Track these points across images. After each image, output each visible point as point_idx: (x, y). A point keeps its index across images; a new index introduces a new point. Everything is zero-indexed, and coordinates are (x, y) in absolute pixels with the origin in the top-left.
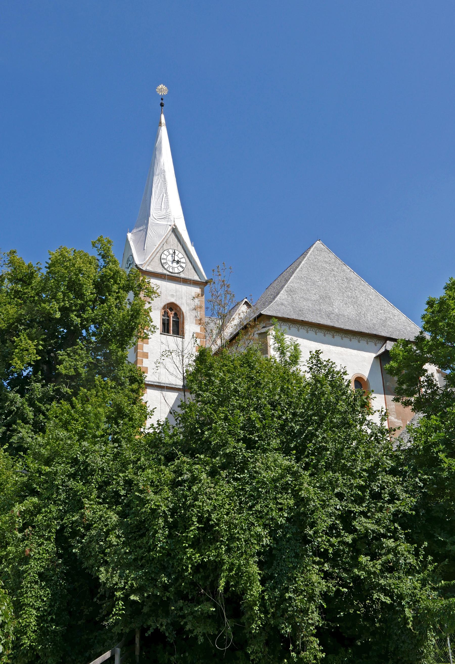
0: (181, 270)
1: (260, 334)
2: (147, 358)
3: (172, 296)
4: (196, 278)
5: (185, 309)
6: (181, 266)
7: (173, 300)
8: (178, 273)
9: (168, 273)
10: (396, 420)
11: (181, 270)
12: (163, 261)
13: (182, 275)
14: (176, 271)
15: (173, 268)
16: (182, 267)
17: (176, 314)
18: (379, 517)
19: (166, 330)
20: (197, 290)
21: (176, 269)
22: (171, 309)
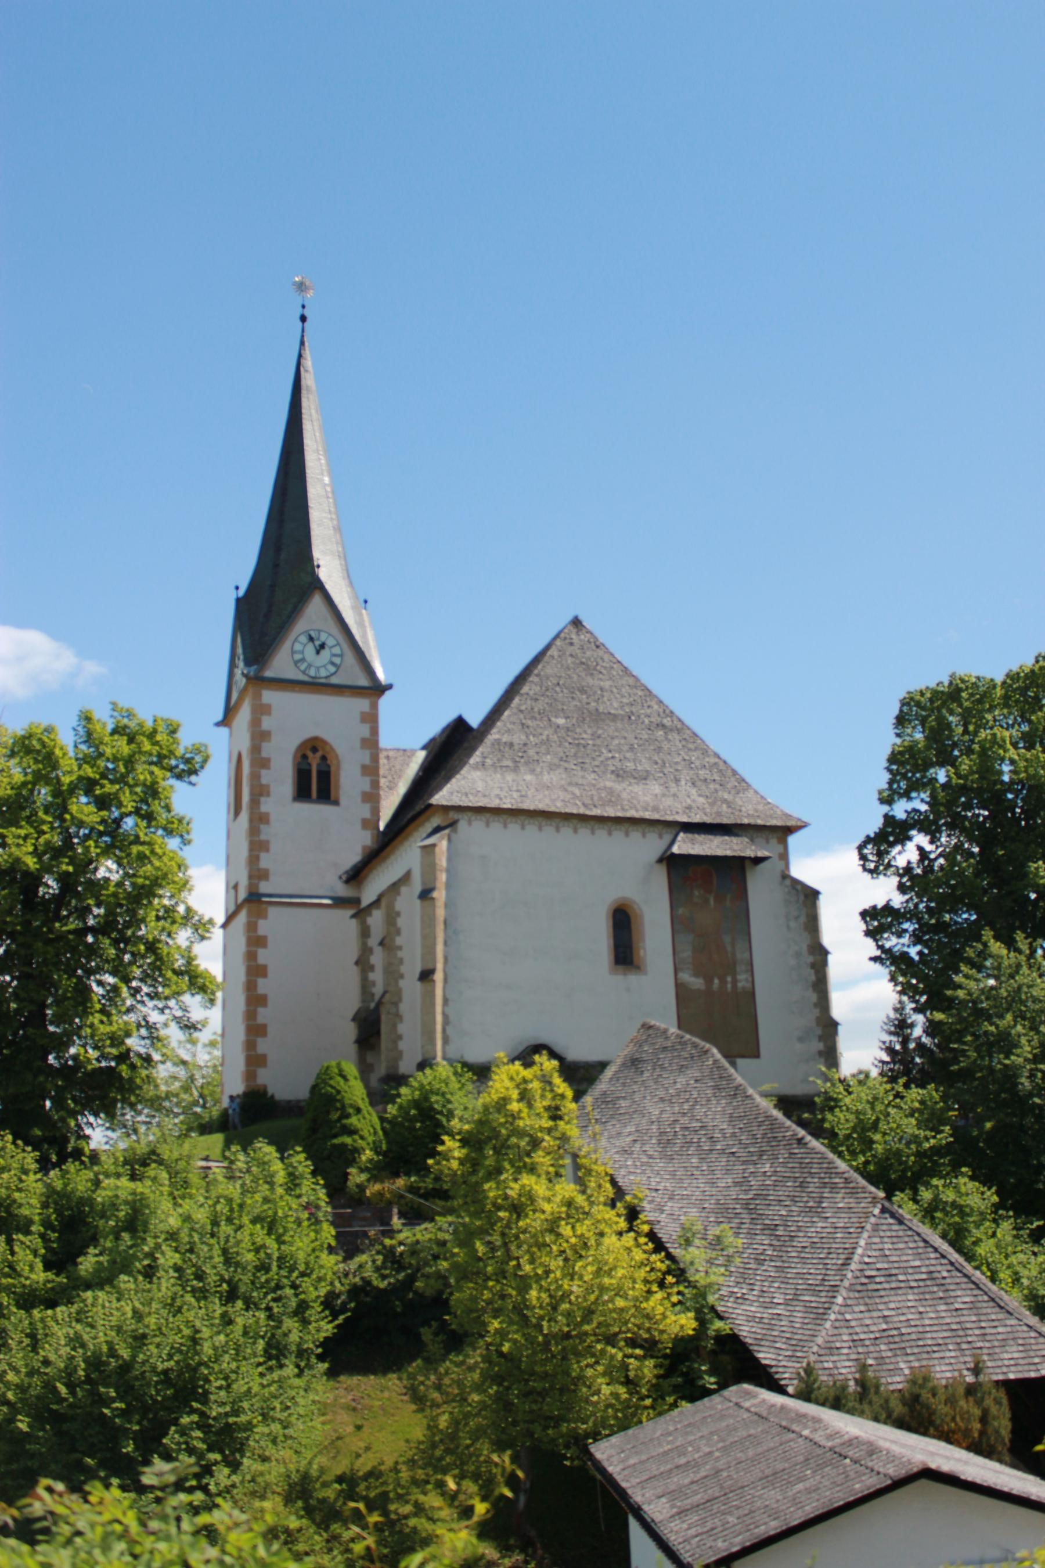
0: (332, 669)
1: (424, 847)
2: (267, 850)
4: (363, 681)
6: (333, 664)
8: (326, 677)
9: (305, 678)
10: (693, 979)
11: (332, 669)
13: (334, 680)
14: (323, 673)
15: (318, 668)
16: (333, 664)
18: (970, 994)
22: (314, 750)
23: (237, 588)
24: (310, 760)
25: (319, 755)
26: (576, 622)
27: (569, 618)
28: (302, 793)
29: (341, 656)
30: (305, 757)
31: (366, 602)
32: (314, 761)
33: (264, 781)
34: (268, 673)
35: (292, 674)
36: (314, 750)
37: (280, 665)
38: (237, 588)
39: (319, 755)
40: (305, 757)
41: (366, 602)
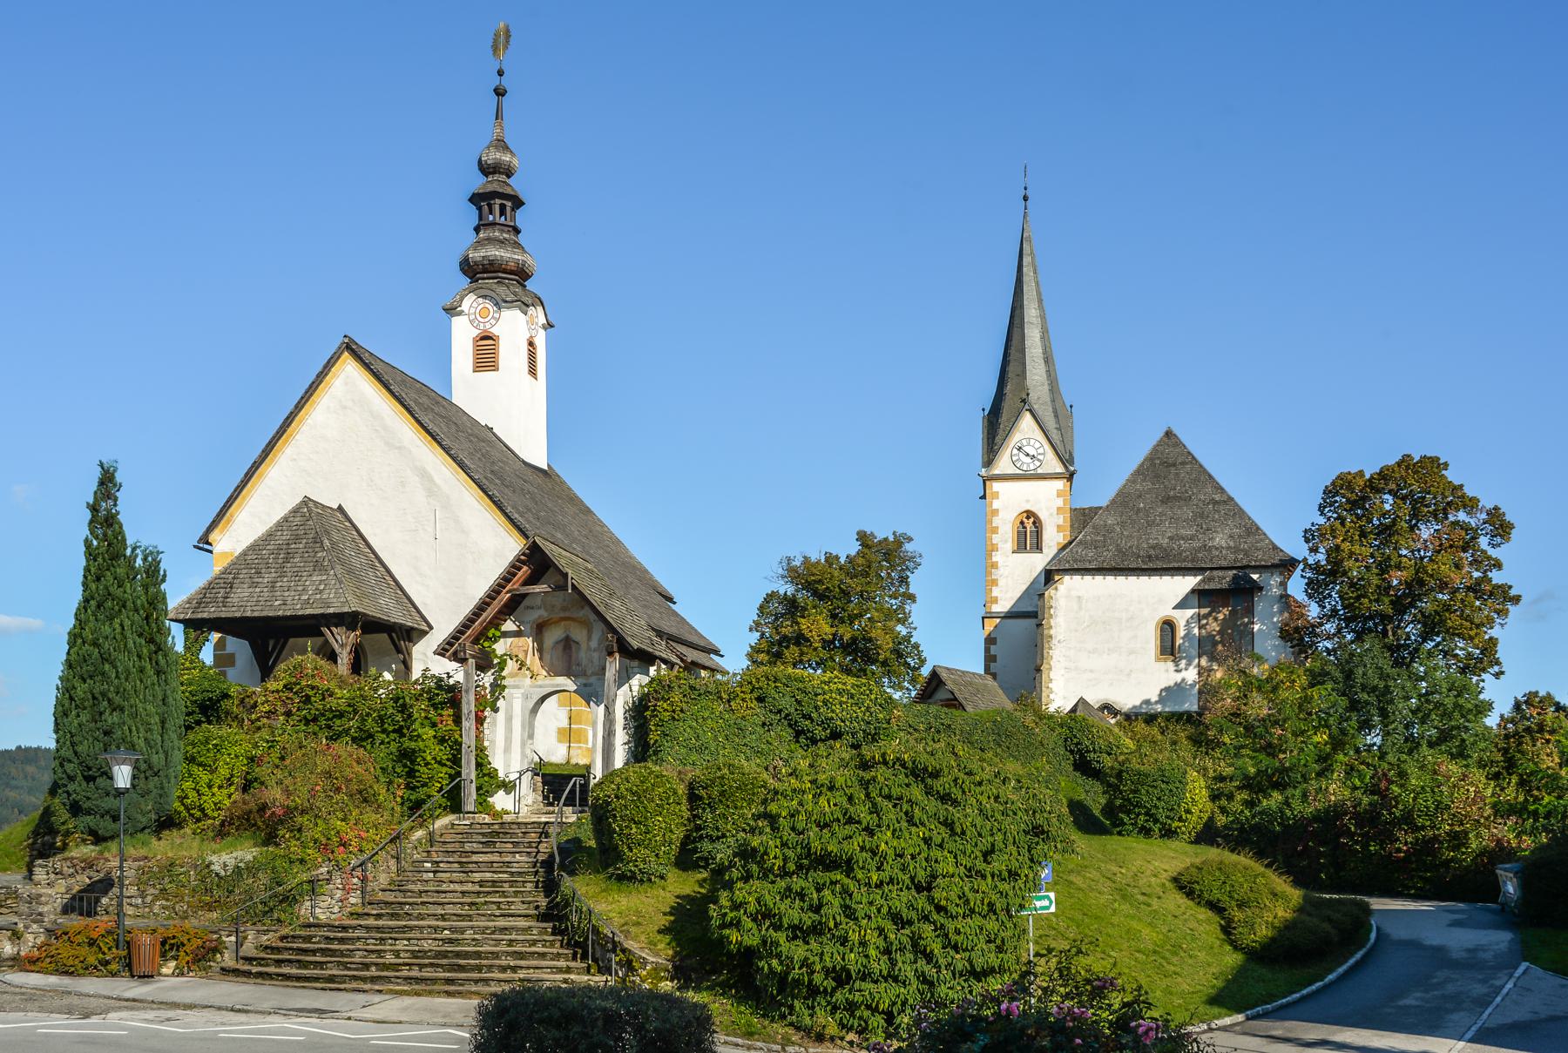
0: (1038, 464)
2: (997, 585)
3: (1028, 501)
5: (1042, 516)
7: (1028, 507)
9: (1021, 472)
11: (1038, 464)
12: (1014, 458)
13: (1040, 471)
14: (1032, 467)
16: (1038, 460)
17: (1034, 523)
19: (1021, 547)
20: (1060, 484)
21: (1028, 465)
22: (1028, 518)
23: (983, 410)
24: (1026, 525)
25: (1032, 520)
26: (1169, 434)
27: (1165, 429)
28: (1021, 547)
29: (1044, 454)
30: (1022, 523)
31: (1071, 407)
32: (1029, 524)
33: (994, 542)
34: (996, 472)
35: (1012, 470)
36: (1028, 518)
37: (1003, 465)
38: (983, 410)
39: (1032, 520)
40: (1022, 523)
41: (1071, 407)
